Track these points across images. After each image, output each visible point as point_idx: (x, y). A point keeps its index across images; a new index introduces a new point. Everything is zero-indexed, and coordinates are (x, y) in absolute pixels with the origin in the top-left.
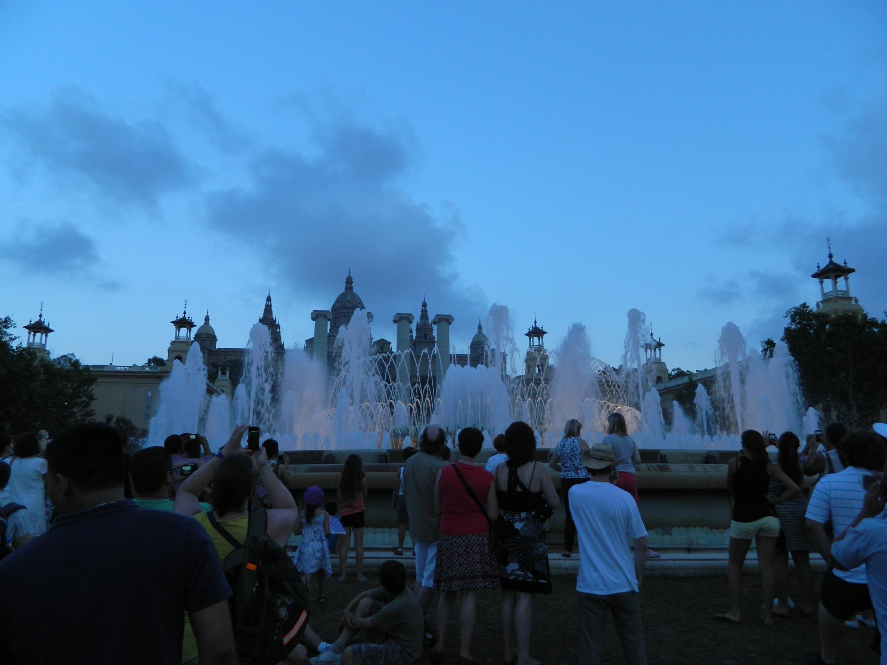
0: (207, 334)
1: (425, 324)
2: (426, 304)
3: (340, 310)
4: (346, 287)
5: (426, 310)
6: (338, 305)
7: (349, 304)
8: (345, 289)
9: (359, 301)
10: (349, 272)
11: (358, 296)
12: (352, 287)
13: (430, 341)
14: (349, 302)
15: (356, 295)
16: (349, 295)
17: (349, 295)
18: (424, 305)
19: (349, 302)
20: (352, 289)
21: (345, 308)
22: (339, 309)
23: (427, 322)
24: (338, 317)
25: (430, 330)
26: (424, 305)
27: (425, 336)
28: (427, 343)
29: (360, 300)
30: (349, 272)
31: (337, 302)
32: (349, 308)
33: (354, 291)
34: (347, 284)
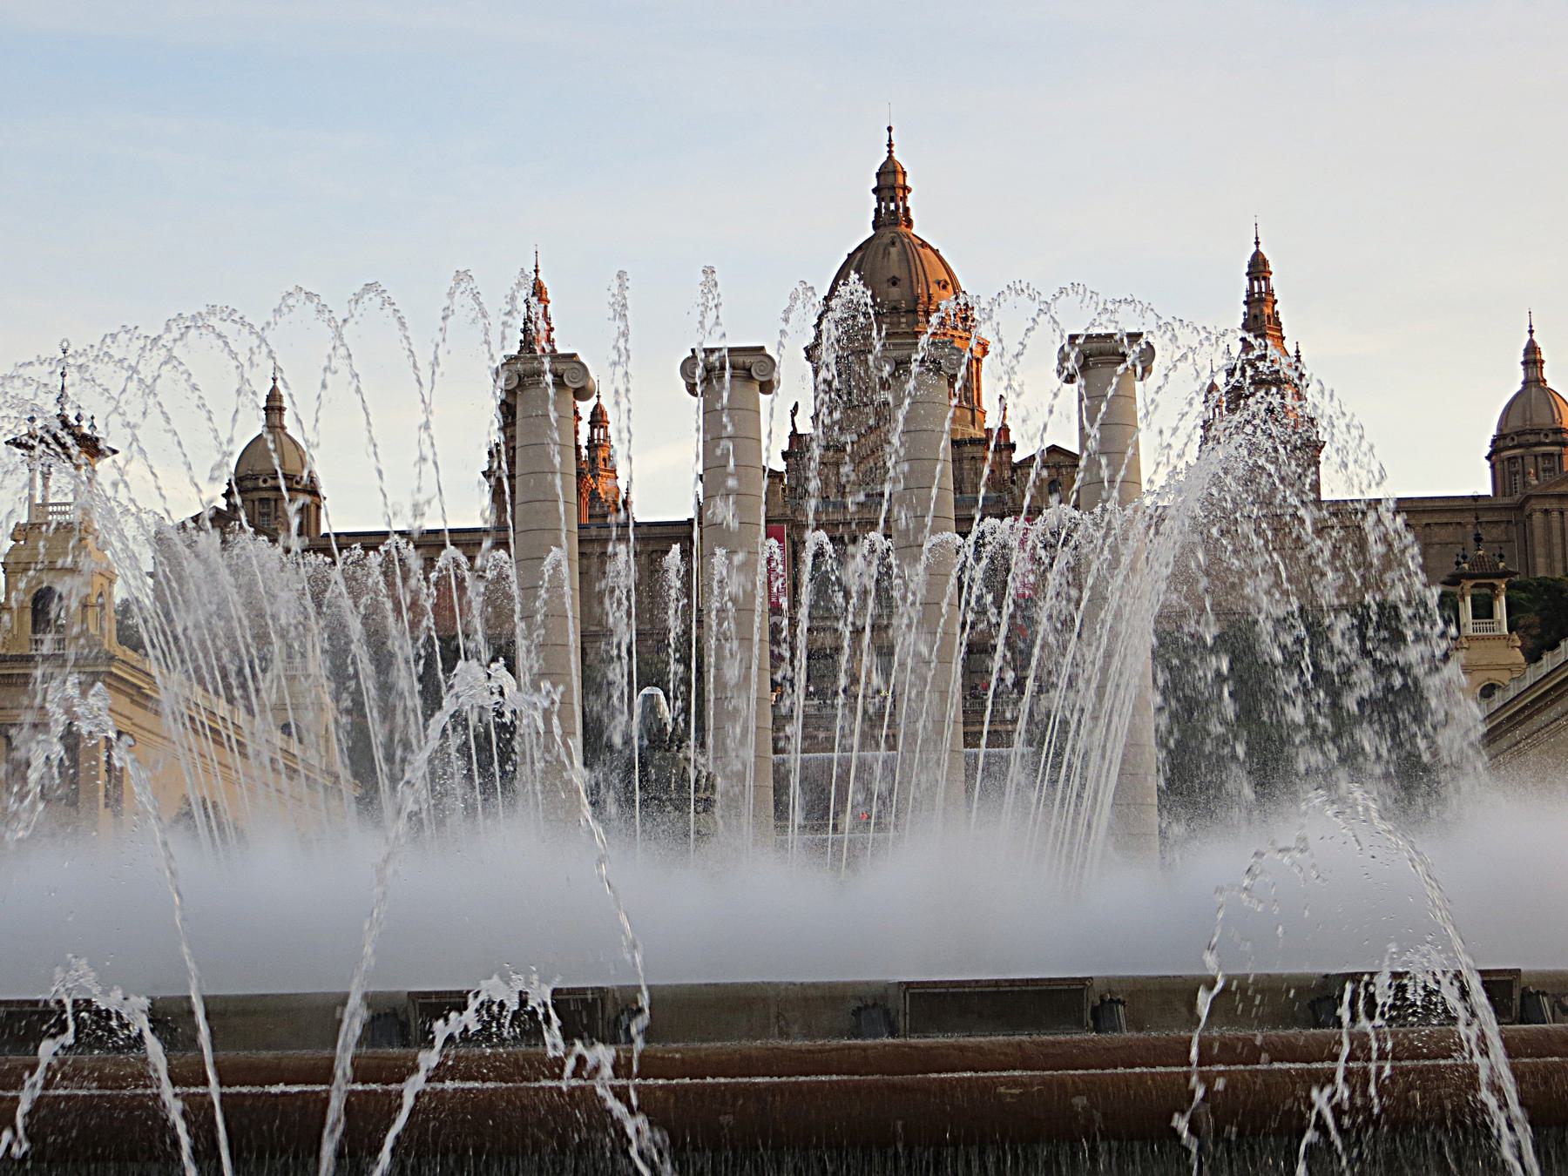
2: (1265, 263)
4: (878, 211)
8: (875, 225)
10: (890, 145)
11: (936, 252)
12: (907, 210)
14: (894, 282)
15: (924, 245)
16: (893, 251)
18: (1258, 268)
19: (894, 282)
20: (909, 223)
26: (1258, 268)
30: (890, 145)
33: (915, 231)
34: (879, 200)
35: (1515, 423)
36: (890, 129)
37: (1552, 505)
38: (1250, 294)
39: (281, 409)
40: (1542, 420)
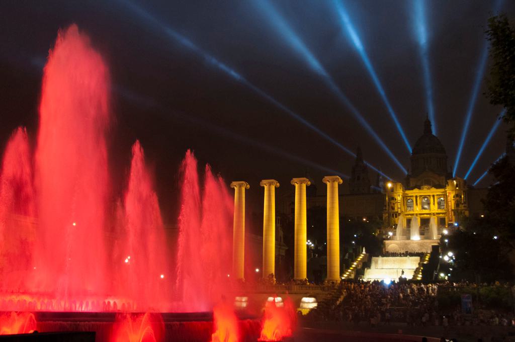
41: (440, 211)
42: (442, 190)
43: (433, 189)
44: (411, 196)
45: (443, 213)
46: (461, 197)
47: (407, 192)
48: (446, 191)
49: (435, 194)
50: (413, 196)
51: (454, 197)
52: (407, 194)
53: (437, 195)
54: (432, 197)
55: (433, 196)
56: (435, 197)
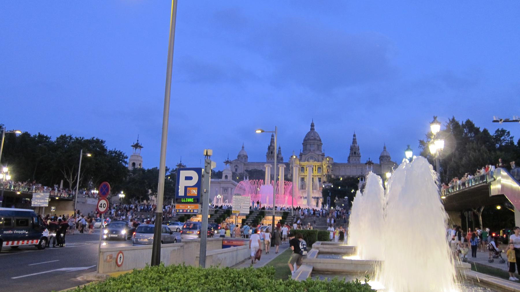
0: (243, 155)
1: (355, 146)
3: (308, 141)
4: (311, 128)
5: (356, 138)
6: (307, 138)
7: (312, 138)
8: (311, 130)
9: (318, 136)
10: (313, 121)
11: (317, 133)
13: (358, 155)
14: (312, 136)
15: (316, 132)
17: (312, 133)
18: (354, 136)
19: (312, 136)
20: (314, 130)
21: (310, 140)
22: (307, 140)
23: (356, 145)
24: (307, 145)
25: (358, 149)
26: (354, 136)
27: (355, 153)
28: (356, 156)
29: (318, 135)
30: (313, 121)
31: (306, 137)
32: (312, 140)
33: (315, 130)
35: (382, 155)
36: (313, 119)
37: (384, 165)
38: (353, 138)
39: (244, 148)
40: (385, 154)
41: (318, 174)
42: (320, 163)
43: (316, 162)
44: (303, 165)
45: (320, 176)
46: (330, 167)
47: (301, 163)
48: (322, 164)
49: (316, 165)
50: (304, 165)
51: (326, 167)
52: (301, 164)
53: (318, 166)
54: (314, 166)
55: (315, 166)
56: (316, 167)
